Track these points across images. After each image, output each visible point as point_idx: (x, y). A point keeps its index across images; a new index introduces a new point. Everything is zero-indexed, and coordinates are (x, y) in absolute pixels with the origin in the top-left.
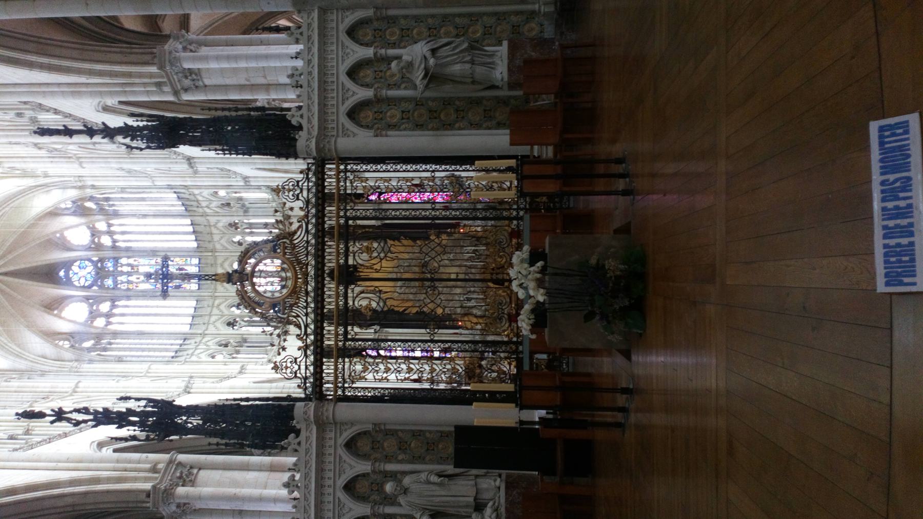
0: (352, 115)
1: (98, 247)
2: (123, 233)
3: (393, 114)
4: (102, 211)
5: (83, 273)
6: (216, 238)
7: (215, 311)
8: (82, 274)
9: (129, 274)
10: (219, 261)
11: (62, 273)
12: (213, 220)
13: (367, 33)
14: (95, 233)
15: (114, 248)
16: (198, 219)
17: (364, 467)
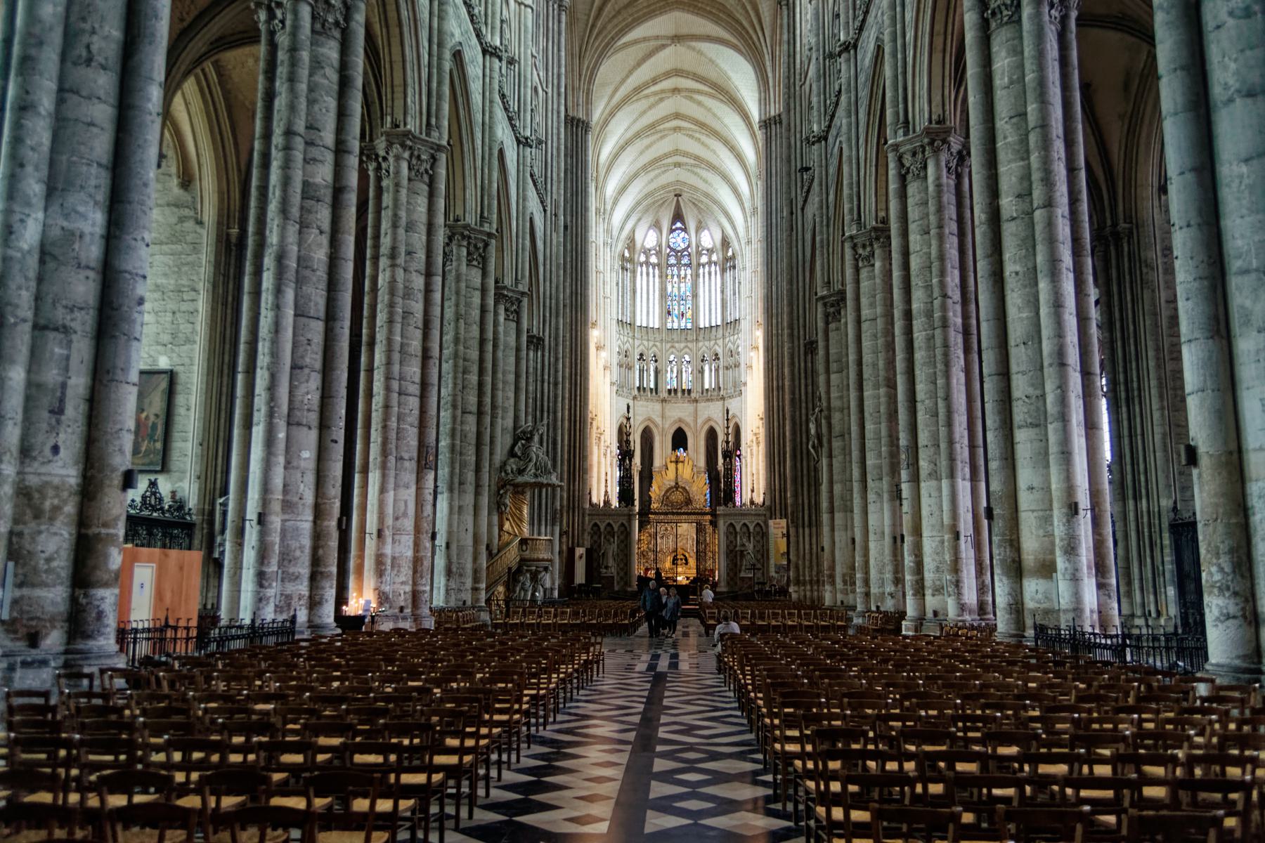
0: (731, 524)
1: (699, 254)
2: (710, 273)
3: (732, 538)
4: (726, 259)
5: (679, 240)
6: (707, 343)
7: (651, 344)
8: (678, 240)
9: (679, 276)
10: (690, 345)
11: (679, 225)
12: (720, 342)
13: (758, 529)
14: (710, 251)
15: (699, 265)
16: (720, 331)
17: (616, 529)
